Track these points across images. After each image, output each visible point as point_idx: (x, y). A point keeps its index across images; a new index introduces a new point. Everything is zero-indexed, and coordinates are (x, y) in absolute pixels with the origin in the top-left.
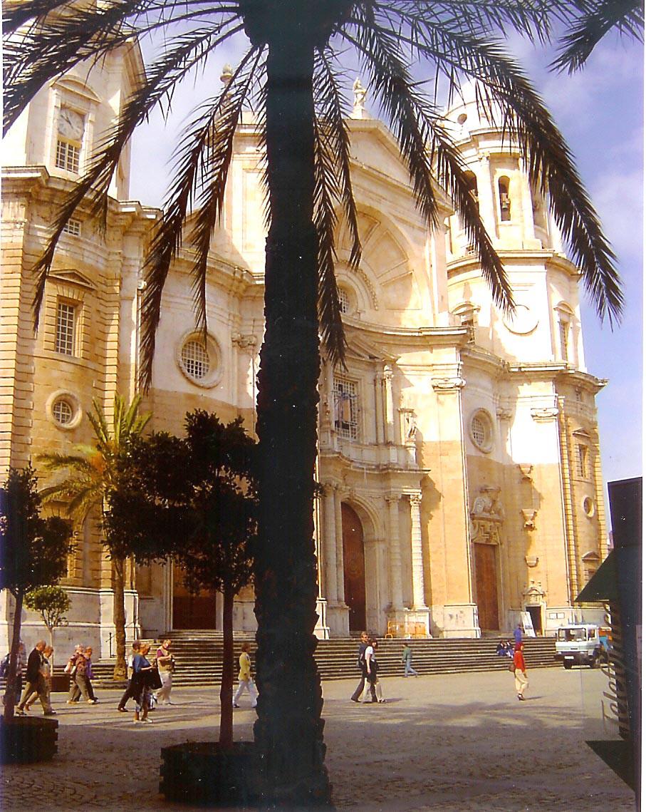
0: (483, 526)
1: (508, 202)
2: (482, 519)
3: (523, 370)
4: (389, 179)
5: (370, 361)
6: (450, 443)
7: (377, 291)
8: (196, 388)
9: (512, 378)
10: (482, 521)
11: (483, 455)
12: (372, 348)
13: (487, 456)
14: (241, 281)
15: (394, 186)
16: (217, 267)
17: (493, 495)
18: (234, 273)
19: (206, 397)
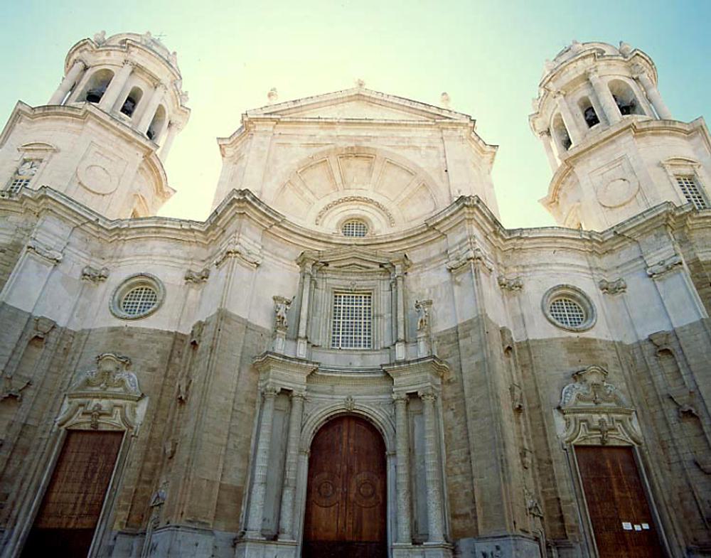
0: (581, 421)
1: (593, 115)
2: (575, 411)
3: (618, 233)
4: (374, 121)
5: (382, 269)
6: (471, 321)
7: (394, 212)
8: (120, 321)
9: (614, 248)
10: (580, 415)
11: (574, 335)
12: (373, 255)
13: (586, 335)
14: (192, 230)
15: (385, 124)
16: (159, 225)
17: (593, 379)
18: (181, 226)
19: (131, 328)
